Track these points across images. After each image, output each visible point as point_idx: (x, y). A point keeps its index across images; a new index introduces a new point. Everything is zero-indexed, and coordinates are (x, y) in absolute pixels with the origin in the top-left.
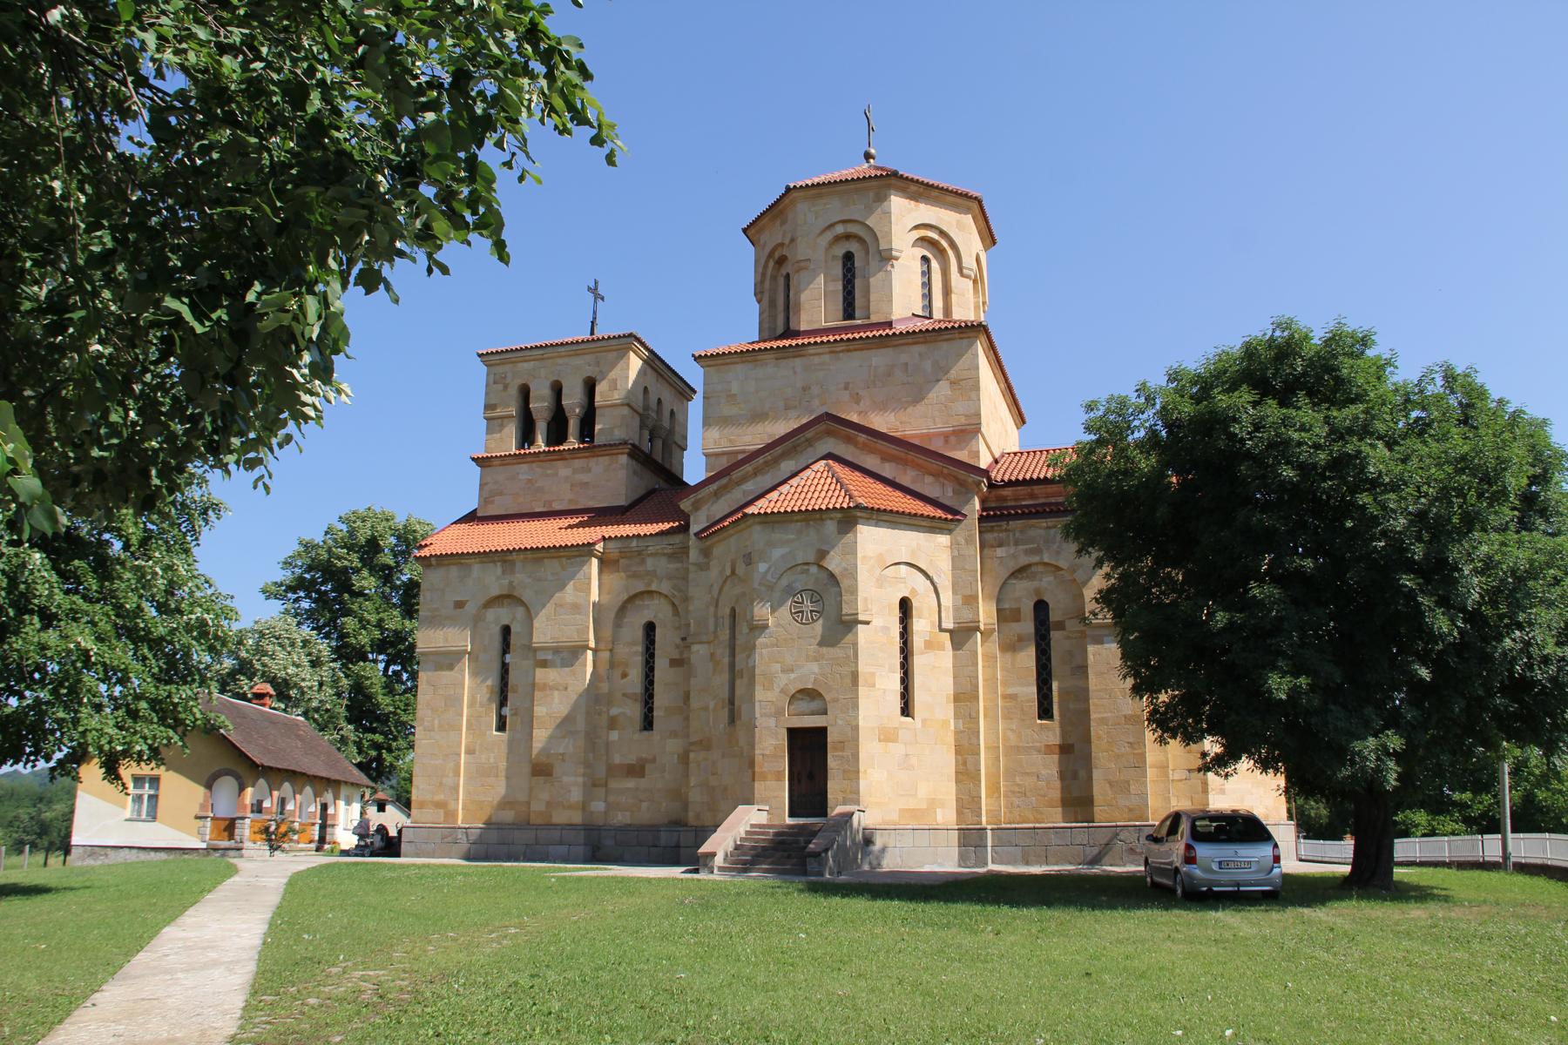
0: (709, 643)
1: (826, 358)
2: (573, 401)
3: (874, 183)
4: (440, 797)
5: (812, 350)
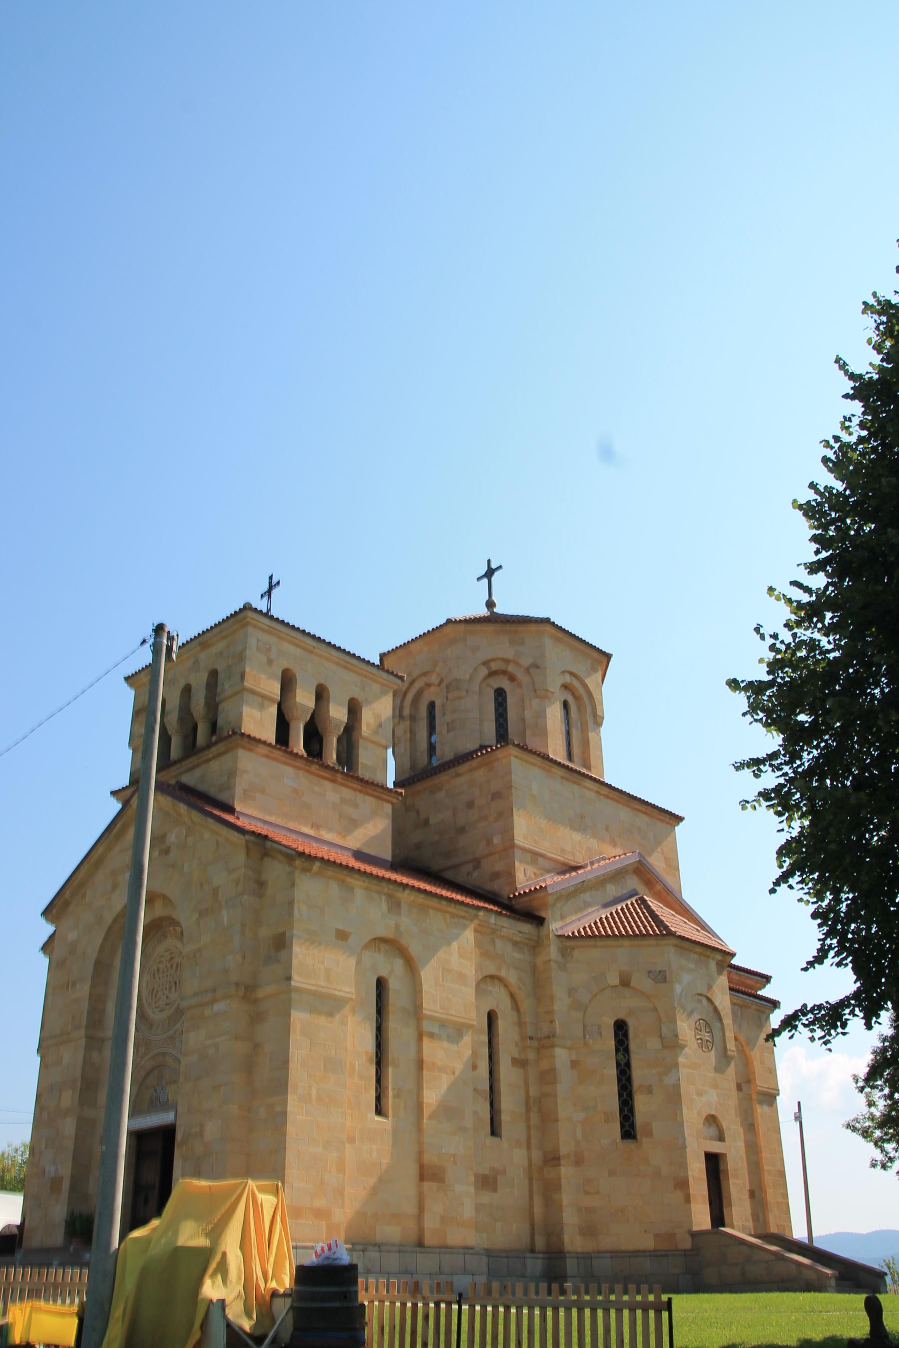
0: (569, 1048)
1: (592, 795)
2: (338, 713)
3: (596, 655)
4: (320, 1203)
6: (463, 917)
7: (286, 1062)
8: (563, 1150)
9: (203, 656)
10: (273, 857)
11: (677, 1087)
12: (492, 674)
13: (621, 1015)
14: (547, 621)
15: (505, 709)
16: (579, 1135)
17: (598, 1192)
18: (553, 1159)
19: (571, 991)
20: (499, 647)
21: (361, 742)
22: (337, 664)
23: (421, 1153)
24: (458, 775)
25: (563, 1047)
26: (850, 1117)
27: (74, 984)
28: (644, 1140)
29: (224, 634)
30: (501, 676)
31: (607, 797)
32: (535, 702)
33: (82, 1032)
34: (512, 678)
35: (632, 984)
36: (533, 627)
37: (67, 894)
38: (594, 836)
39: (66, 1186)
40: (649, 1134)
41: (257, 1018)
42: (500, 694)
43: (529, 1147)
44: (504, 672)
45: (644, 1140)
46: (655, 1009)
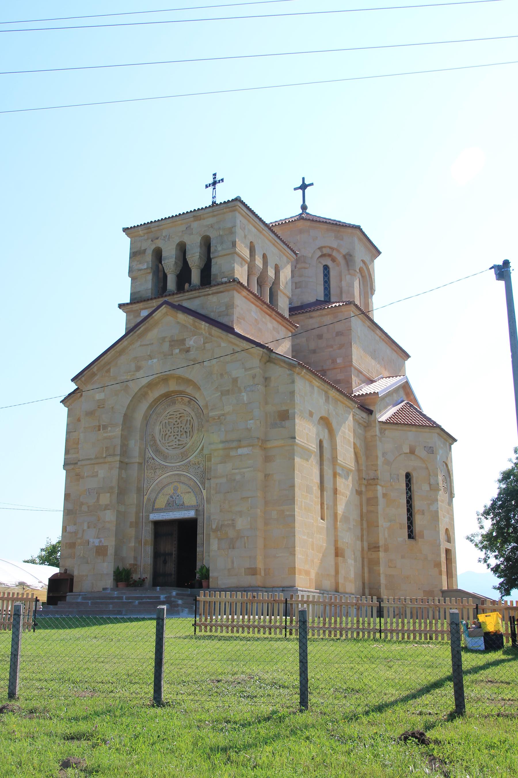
1: (377, 338)
5: (378, 331)
6: (349, 407)
7: (293, 486)
8: (381, 543)
9: (195, 225)
10: (275, 363)
11: (437, 512)
12: (323, 256)
13: (409, 470)
14: (358, 228)
15: (329, 279)
16: (386, 535)
17: (395, 567)
18: (374, 547)
19: (384, 454)
20: (329, 240)
21: (279, 293)
22: (271, 242)
23: (336, 541)
24: (311, 317)
25: (380, 485)
26: (469, 534)
27: (105, 427)
28: (419, 540)
29: (215, 213)
30: (327, 258)
31: (383, 340)
32: (348, 277)
33: (118, 458)
34: (334, 260)
35: (416, 453)
36: (350, 230)
37: (95, 369)
38: (379, 363)
39: (111, 551)
40: (422, 536)
41: (267, 459)
42: (326, 268)
43: (362, 541)
44: (330, 255)
45: (419, 540)
46: (427, 468)
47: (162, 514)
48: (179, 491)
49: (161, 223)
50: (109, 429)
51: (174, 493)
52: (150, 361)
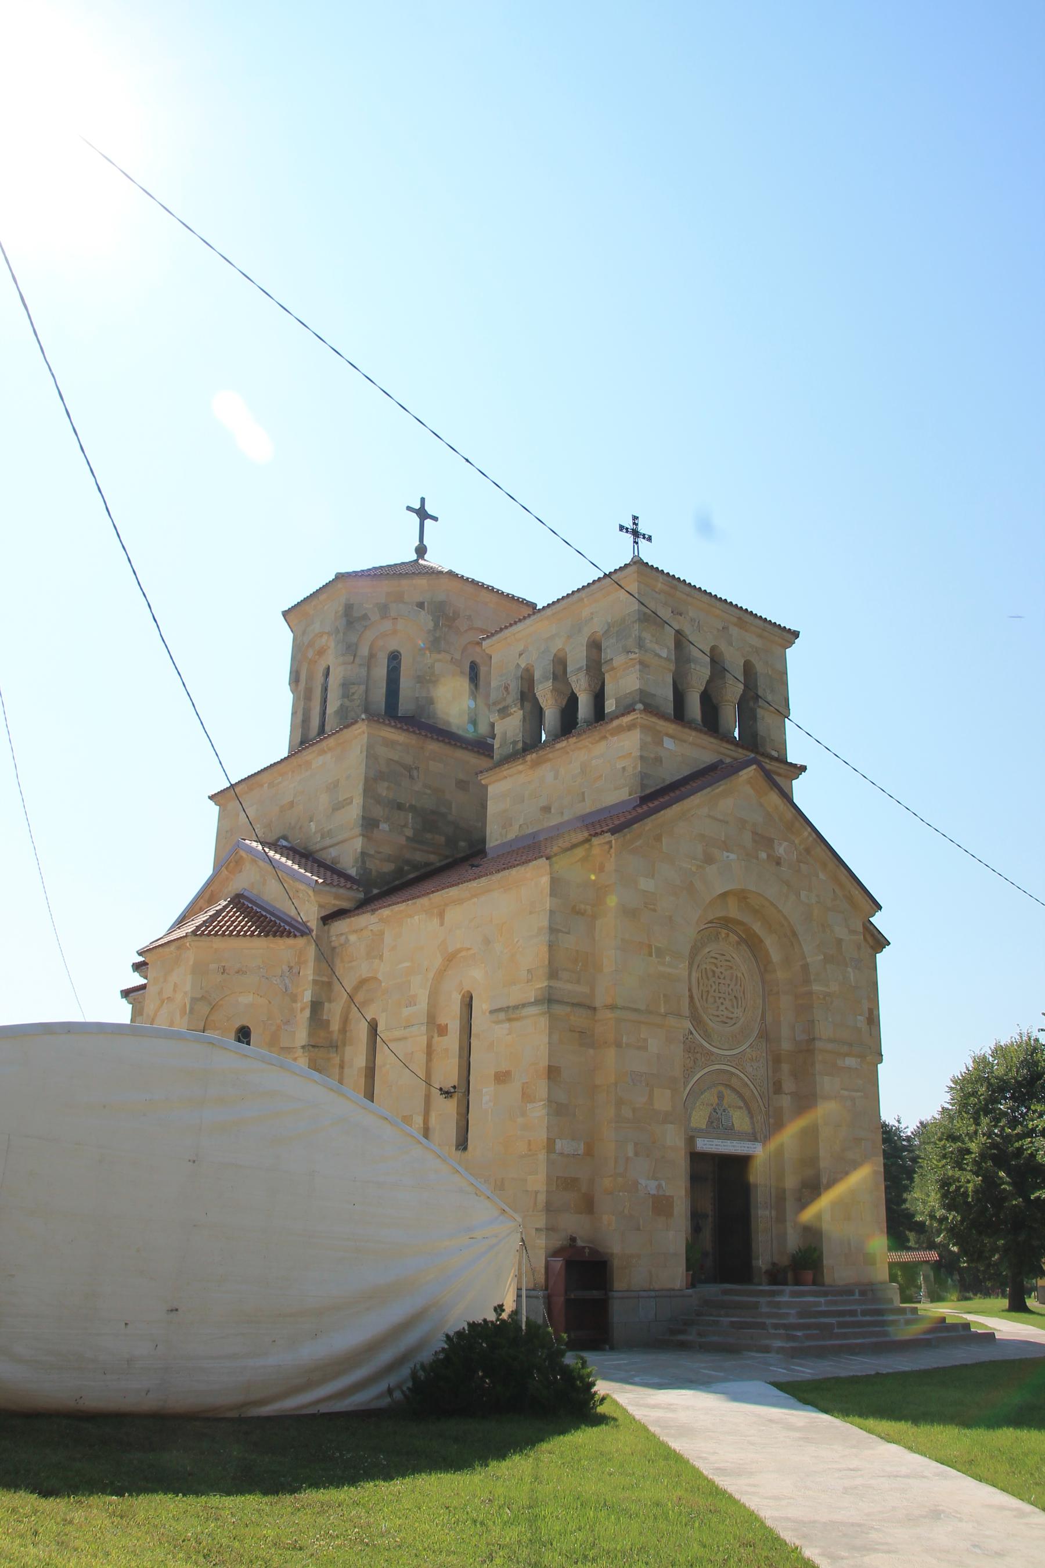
47: (716, 1142)
48: (725, 1102)
49: (694, 592)
50: (668, 959)
51: (718, 1104)
52: (726, 854)
